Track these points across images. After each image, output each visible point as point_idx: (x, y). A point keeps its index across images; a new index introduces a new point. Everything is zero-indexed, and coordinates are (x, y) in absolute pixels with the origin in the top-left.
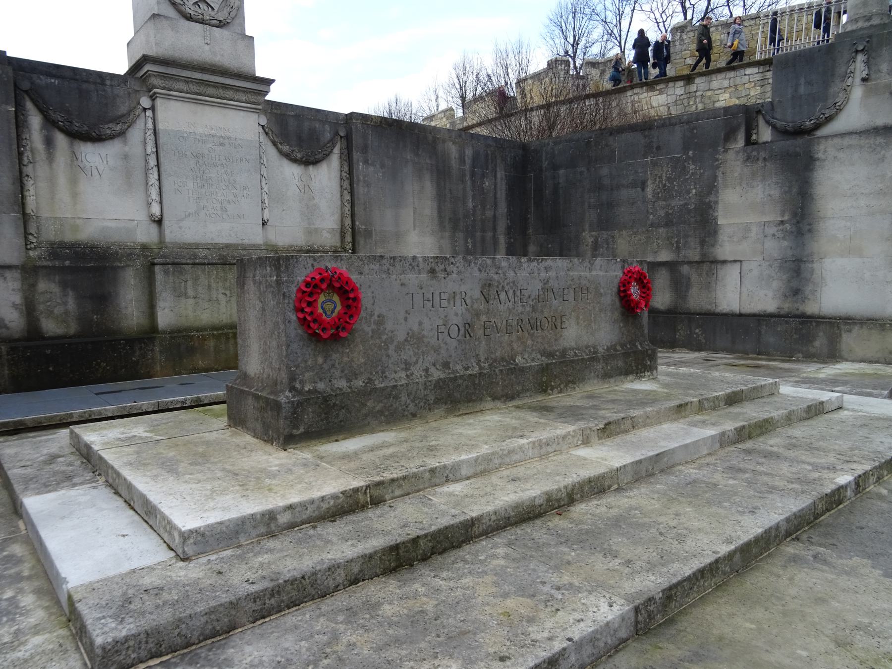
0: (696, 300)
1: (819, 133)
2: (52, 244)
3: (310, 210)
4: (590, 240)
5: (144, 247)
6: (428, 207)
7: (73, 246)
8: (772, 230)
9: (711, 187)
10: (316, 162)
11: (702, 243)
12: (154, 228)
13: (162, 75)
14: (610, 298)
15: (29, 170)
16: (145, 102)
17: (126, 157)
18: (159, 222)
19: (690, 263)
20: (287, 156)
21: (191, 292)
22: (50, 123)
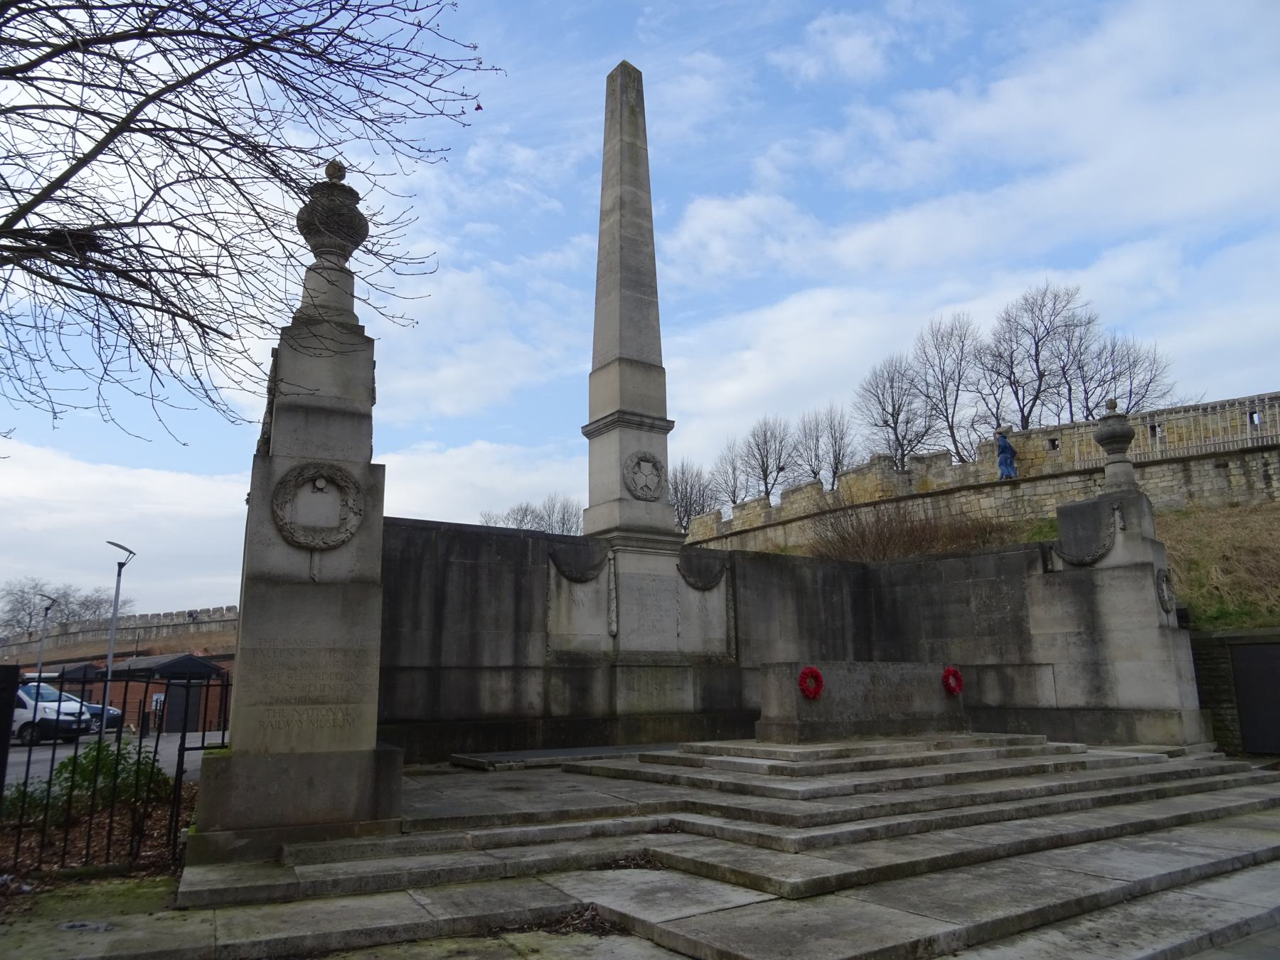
0: (1021, 697)
1: (1098, 566)
4: (927, 646)
5: (605, 654)
7: (568, 653)
8: (1073, 639)
9: (1022, 605)
11: (1020, 649)
12: (611, 640)
13: (624, 538)
14: (938, 685)
16: (610, 555)
17: (597, 592)
18: (614, 636)
19: (1013, 666)
21: (636, 687)
22: (561, 572)
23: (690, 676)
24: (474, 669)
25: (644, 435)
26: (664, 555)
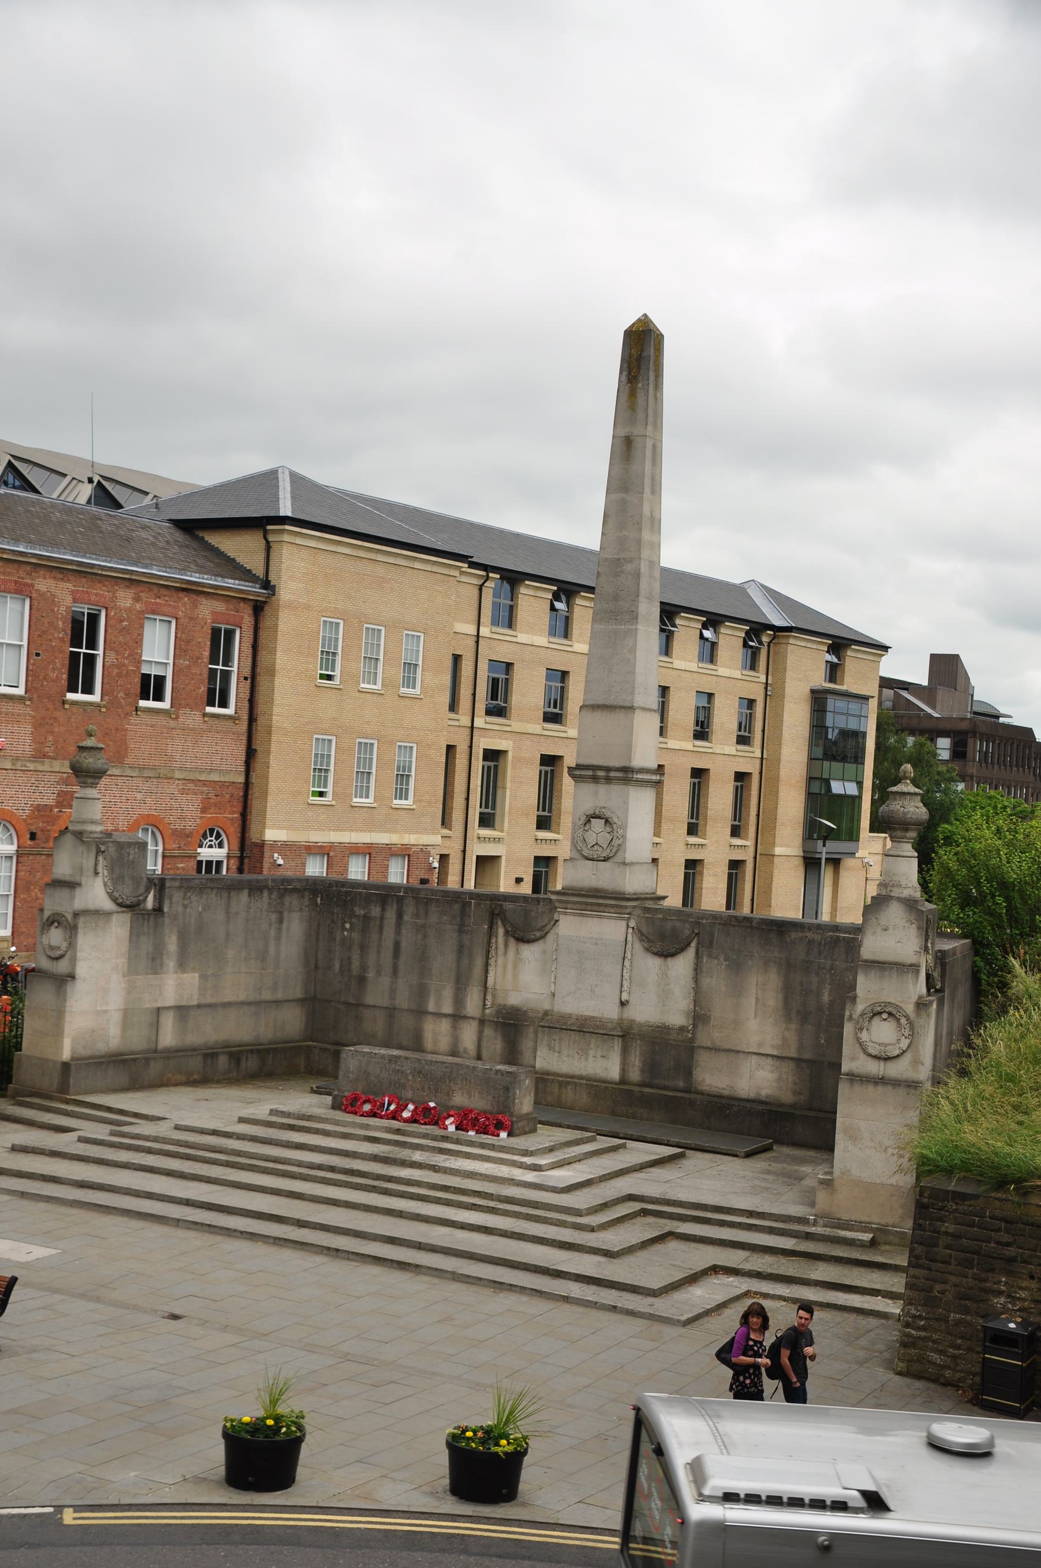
2: (500, 1005)
3: (665, 994)
6: (773, 999)
10: (673, 955)
13: (559, 901)
15: (492, 961)
17: (544, 952)
20: (647, 950)
21: (557, 1049)
22: (507, 933)
23: (617, 1045)
24: (420, 1012)
25: (602, 788)
26: (608, 918)
